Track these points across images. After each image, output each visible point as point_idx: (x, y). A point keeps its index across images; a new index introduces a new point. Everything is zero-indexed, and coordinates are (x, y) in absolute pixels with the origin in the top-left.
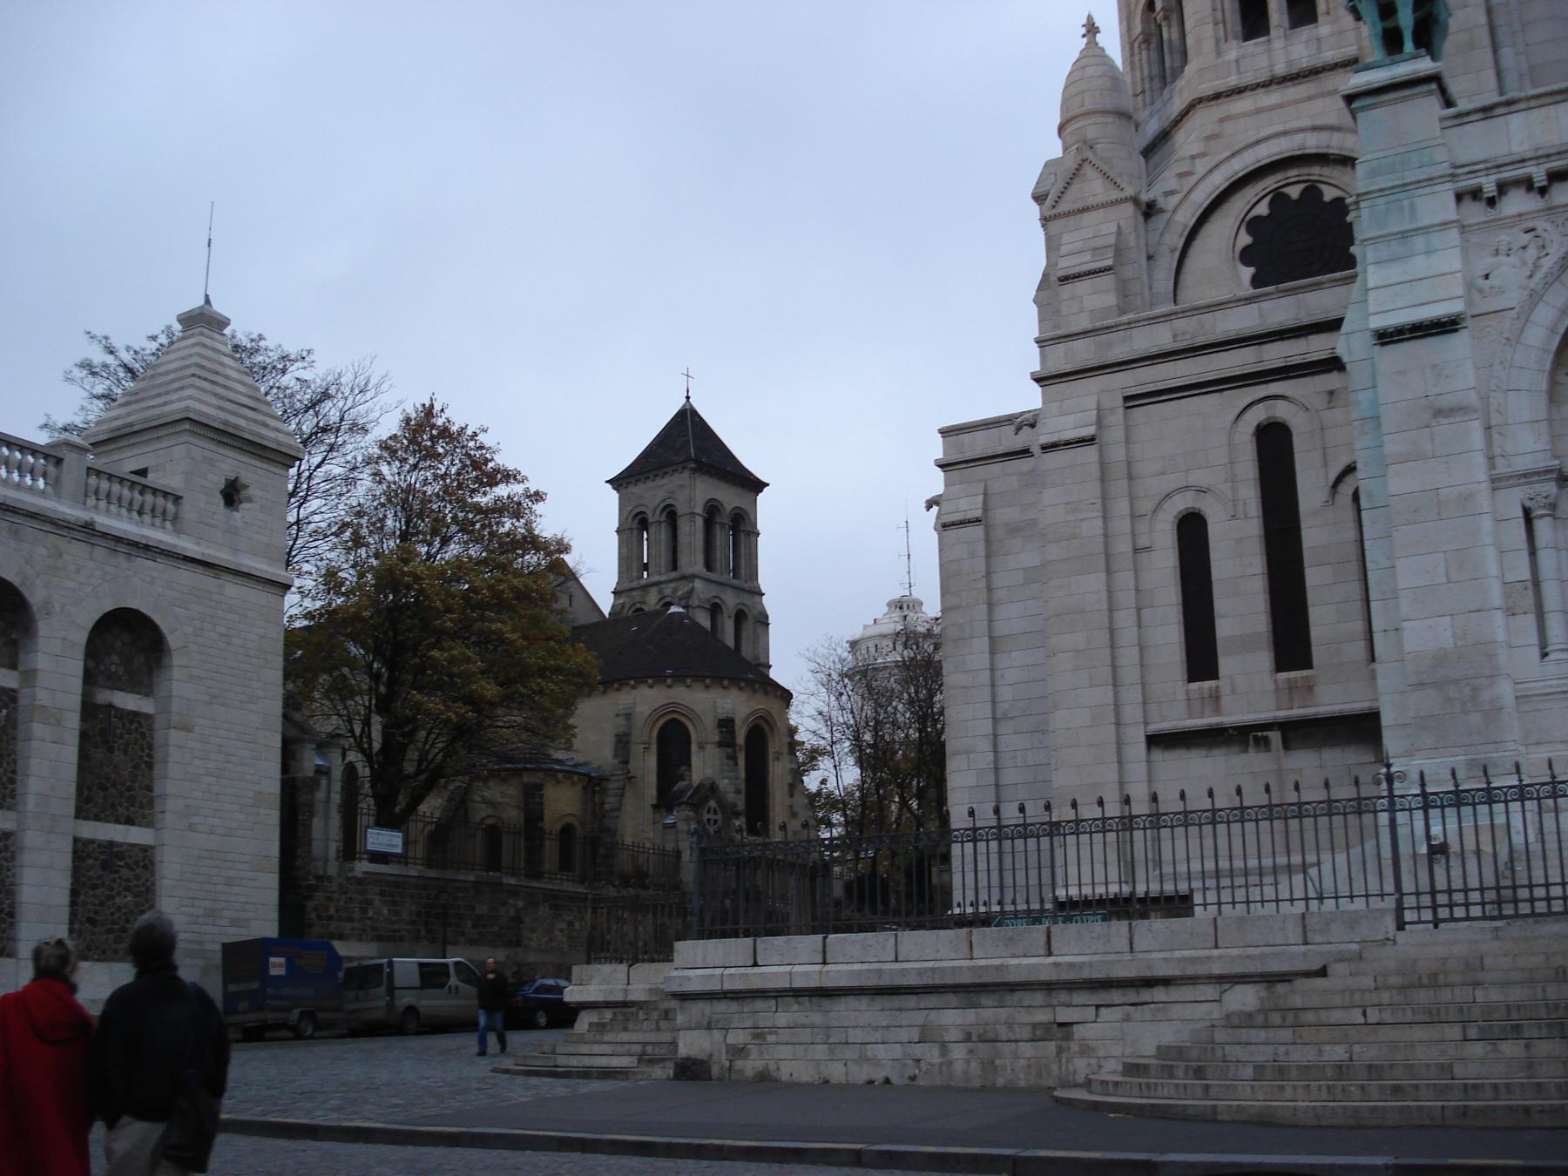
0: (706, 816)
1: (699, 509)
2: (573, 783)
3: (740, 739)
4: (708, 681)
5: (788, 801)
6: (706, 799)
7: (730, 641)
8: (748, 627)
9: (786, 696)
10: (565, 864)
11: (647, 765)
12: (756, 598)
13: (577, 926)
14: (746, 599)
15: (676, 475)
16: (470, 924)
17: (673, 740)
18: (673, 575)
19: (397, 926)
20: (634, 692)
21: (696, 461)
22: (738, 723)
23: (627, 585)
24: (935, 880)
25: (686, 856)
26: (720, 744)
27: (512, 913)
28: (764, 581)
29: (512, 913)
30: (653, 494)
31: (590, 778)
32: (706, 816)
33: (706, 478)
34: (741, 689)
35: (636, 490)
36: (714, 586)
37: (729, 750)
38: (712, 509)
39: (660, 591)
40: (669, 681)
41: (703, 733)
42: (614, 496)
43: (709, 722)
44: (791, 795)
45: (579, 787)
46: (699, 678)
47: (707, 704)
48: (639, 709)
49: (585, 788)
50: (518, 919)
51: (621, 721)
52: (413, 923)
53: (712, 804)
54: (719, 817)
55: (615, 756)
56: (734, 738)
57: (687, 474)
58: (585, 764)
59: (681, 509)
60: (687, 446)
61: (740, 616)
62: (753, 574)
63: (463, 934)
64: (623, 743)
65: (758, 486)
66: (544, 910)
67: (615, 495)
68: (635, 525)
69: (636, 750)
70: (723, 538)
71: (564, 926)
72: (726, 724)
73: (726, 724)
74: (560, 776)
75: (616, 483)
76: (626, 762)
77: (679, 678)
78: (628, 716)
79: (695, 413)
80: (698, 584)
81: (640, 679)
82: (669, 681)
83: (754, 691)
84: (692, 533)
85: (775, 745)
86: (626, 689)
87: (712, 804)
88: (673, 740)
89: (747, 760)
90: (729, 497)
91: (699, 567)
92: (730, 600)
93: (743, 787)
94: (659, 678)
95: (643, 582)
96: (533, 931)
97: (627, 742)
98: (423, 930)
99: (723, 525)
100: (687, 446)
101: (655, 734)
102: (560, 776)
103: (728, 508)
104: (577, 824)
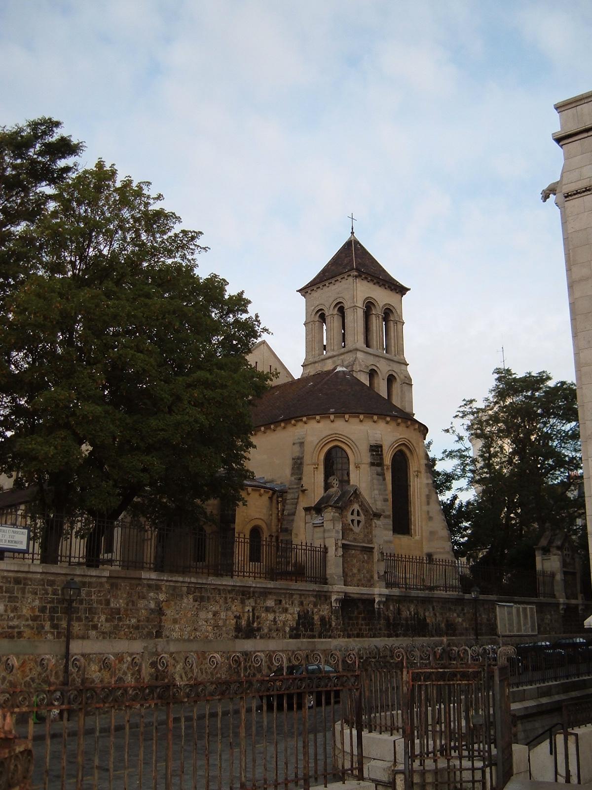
0: (350, 517)
1: (360, 304)
2: (261, 495)
3: (388, 460)
4: (362, 417)
5: (425, 508)
6: (351, 502)
7: (385, 395)
8: (396, 387)
9: (424, 430)
10: (255, 556)
11: (315, 482)
12: (403, 367)
13: (223, 615)
14: (396, 367)
15: (344, 281)
16: (103, 618)
17: (334, 461)
18: (343, 350)
19: (15, 623)
20: (306, 425)
21: (357, 270)
22: (385, 448)
23: (311, 360)
24: (539, 567)
25: (331, 551)
26: (372, 464)
27: (152, 605)
28: (408, 356)
29: (152, 605)
30: (327, 296)
31: (274, 491)
32: (350, 517)
33: (365, 282)
34: (387, 423)
35: (315, 294)
36: (372, 357)
37: (379, 469)
38: (369, 305)
39: (334, 362)
40: (332, 417)
42: (302, 300)
44: (428, 503)
45: (265, 498)
46: (355, 414)
47: (360, 433)
48: (309, 439)
49: (271, 498)
50: (160, 612)
51: (297, 448)
52: (35, 619)
53: (356, 507)
54: (362, 518)
55: (292, 474)
56: (382, 459)
57: (351, 279)
58: (272, 481)
59: (346, 306)
60: (353, 261)
61: (391, 379)
62: (401, 350)
63: (95, 627)
64: (298, 465)
66: (188, 602)
67: (303, 299)
68: (317, 318)
69: (307, 469)
70: (377, 323)
71: (210, 615)
72: (376, 450)
73: (376, 450)
74: (250, 489)
75: (304, 291)
76: (300, 479)
77: (340, 414)
78: (302, 444)
79: (357, 243)
80: (360, 355)
81: (310, 415)
82: (332, 417)
83: (398, 424)
84: (355, 320)
85: (415, 465)
86: (300, 424)
87: (356, 507)
88: (334, 461)
90: (382, 297)
91: (361, 344)
92: (384, 369)
93: (390, 497)
94: (324, 413)
95: (322, 357)
96: (175, 621)
97: (301, 464)
98: (47, 627)
99: (377, 316)
100: (353, 261)
101: (322, 457)
102: (250, 489)
103: (381, 304)
104: (264, 526)
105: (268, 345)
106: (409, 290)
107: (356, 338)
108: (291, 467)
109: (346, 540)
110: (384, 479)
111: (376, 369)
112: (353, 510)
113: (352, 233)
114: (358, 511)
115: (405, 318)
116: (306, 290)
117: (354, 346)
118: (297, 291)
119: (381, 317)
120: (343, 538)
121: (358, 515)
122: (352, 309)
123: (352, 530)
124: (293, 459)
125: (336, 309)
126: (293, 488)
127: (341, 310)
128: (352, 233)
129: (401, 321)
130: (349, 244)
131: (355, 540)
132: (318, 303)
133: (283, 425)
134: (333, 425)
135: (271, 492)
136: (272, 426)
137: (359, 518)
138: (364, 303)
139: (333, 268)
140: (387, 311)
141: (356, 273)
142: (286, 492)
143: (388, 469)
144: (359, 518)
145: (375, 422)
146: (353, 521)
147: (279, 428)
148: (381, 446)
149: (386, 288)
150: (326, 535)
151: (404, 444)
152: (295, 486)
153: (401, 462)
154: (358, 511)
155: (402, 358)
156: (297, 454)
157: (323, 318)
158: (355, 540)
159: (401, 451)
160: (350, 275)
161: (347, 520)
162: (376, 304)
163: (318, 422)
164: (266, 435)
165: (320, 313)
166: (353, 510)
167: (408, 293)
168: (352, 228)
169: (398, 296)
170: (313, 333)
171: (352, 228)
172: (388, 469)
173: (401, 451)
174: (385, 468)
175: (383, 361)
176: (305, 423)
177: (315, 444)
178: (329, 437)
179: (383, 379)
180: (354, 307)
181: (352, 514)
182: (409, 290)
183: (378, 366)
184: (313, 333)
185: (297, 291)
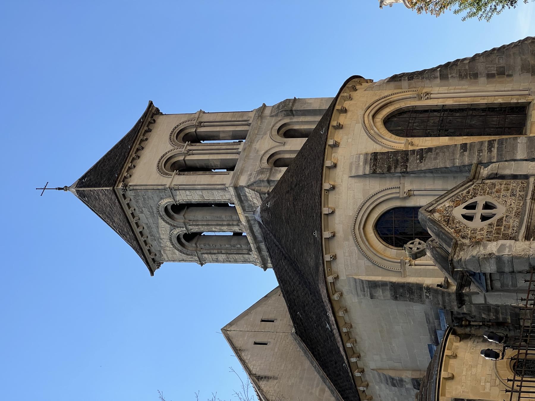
1: (167, 181)
2: (455, 357)
3: (399, 143)
5: (482, 80)
12: (267, 112)
20: (342, 277)
37: (411, 159)
41: (392, 192)
43: (375, 186)
49: (464, 337)
51: (379, 293)
59: (167, 201)
65: (152, 114)
70: (198, 154)
75: (153, 263)
86: (339, 285)
89: (427, 135)
90: (160, 144)
92: (266, 144)
101: (392, 252)
103: (169, 147)
105: (230, 324)
106: (151, 104)
107: (216, 186)
108: (408, 302)
109: (518, 232)
110: (430, 150)
111: (268, 156)
112: (464, 216)
113: (66, 188)
114: (466, 208)
115: (194, 110)
116: (150, 261)
117: (232, 190)
118: (152, 274)
119: (189, 148)
120: (515, 238)
121: (472, 207)
122: (174, 192)
123: (500, 220)
124: (396, 298)
125: (176, 215)
126: (444, 302)
127: (178, 208)
128: (66, 188)
129: (197, 116)
130: (82, 196)
131: (519, 214)
132: (169, 244)
133: (341, 314)
134: (340, 234)
135: (451, 337)
136: (345, 330)
137: (480, 206)
138: (167, 174)
139: (116, 220)
140: (182, 135)
141: (120, 186)
142: (452, 312)
143: (412, 144)
144: (480, 206)
145: (335, 166)
146: (484, 218)
147: (347, 318)
148: (375, 154)
149: (147, 139)
150: (507, 269)
151: (374, 116)
152: (440, 298)
153: (401, 122)
154: (466, 208)
155: (252, 115)
156: (388, 294)
157: (190, 237)
158: (519, 214)
159: (387, 122)
160: (124, 195)
161: (482, 229)
162: (169, 155)
163: (335, 257)
164: (358, 340)
165: (183, 241)
166: (464, 216)
167: (156, 105)
168: (59, 189)
169: (160, 120)
170: (216, 251)
171: (59, 189)
172: (412, 144)
173: (387, 122)
174: (410, 148)
175: (257, 145)
176: (337, 278)
177: (370, 264)
178: (359, 240)
179: (284, 144)
180: (171, 189)
181: (469, 218)
182: (151, 104)
183: (263, 152)
184: (216, 251)
185: (152, 274)
